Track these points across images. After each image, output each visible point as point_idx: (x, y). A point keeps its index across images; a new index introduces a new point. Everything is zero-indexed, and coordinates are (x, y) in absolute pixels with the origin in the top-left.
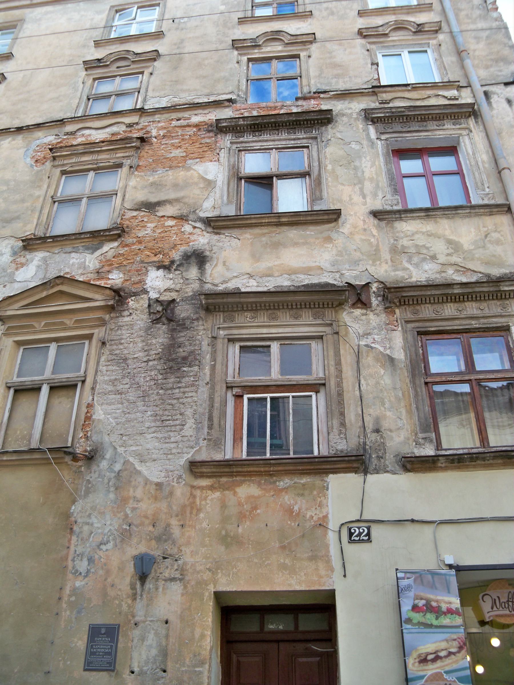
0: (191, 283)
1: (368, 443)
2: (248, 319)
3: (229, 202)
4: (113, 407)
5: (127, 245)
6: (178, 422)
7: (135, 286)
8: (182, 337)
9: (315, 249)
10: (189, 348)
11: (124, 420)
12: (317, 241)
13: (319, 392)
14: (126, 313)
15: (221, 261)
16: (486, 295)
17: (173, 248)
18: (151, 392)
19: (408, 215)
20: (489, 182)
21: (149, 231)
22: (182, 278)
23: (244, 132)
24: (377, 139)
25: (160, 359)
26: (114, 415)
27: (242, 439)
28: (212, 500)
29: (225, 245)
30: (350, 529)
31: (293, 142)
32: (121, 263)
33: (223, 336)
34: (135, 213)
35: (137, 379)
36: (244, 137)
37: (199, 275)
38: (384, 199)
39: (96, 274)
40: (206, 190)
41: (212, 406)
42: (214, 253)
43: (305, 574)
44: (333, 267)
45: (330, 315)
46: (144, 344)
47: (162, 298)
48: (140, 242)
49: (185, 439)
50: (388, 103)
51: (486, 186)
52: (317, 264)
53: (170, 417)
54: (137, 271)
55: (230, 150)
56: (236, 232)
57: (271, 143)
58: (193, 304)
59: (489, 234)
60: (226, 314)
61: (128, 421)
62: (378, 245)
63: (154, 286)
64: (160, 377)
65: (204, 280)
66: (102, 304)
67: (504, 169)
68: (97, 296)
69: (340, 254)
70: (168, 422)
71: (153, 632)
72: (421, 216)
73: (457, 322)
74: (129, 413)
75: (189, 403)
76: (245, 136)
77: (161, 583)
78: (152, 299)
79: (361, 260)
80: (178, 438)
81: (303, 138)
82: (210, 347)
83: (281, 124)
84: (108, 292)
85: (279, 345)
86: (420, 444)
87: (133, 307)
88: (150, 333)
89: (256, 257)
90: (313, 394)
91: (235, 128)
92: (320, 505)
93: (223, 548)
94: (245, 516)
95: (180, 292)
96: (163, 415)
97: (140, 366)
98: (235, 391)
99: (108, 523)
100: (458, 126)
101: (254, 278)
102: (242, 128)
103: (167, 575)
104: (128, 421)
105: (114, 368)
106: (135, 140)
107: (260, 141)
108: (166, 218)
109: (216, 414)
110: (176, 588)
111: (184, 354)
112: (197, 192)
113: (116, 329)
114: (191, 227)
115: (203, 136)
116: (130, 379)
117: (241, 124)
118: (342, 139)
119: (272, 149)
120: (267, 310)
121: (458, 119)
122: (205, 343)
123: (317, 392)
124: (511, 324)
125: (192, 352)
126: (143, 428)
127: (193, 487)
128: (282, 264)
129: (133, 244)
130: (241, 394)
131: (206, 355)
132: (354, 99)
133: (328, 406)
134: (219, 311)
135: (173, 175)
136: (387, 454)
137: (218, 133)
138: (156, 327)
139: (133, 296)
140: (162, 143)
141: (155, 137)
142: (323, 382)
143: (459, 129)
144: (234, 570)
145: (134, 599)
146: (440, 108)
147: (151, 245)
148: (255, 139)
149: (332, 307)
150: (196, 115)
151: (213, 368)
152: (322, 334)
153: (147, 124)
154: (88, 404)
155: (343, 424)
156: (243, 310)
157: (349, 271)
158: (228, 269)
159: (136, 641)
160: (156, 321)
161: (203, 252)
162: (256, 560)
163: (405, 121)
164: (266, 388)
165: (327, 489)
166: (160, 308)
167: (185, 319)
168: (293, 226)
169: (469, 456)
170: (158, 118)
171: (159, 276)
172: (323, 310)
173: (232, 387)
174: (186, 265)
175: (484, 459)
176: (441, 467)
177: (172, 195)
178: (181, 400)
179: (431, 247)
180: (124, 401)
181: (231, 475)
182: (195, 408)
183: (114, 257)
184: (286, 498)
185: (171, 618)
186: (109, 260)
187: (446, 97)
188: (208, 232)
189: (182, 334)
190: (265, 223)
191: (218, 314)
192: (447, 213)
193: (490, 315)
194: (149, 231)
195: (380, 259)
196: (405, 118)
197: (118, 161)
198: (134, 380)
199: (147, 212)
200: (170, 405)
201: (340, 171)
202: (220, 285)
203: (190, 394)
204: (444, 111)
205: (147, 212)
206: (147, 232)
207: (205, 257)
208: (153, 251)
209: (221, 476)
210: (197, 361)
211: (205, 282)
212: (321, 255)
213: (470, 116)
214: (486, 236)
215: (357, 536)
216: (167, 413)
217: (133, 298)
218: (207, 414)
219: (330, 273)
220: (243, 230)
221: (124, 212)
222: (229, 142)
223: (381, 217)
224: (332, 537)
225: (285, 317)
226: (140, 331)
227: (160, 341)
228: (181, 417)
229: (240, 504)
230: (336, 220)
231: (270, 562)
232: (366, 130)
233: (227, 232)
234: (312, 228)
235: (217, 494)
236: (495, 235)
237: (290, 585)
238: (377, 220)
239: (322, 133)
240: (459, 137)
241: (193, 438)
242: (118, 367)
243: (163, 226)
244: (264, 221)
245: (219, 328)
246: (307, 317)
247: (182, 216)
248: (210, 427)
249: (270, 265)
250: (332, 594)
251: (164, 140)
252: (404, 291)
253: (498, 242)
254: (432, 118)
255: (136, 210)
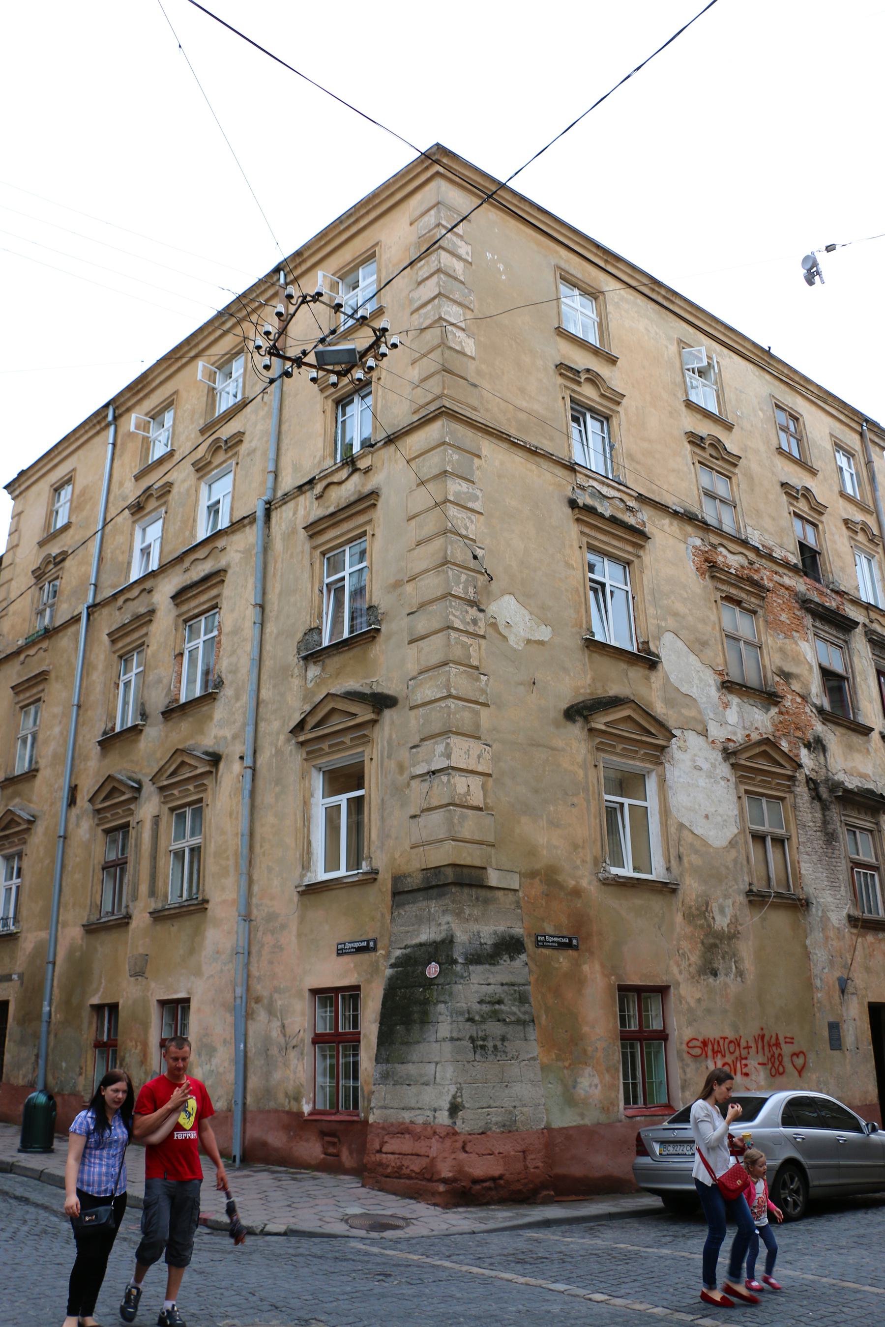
56: (833, 727)
148: (822, 627)
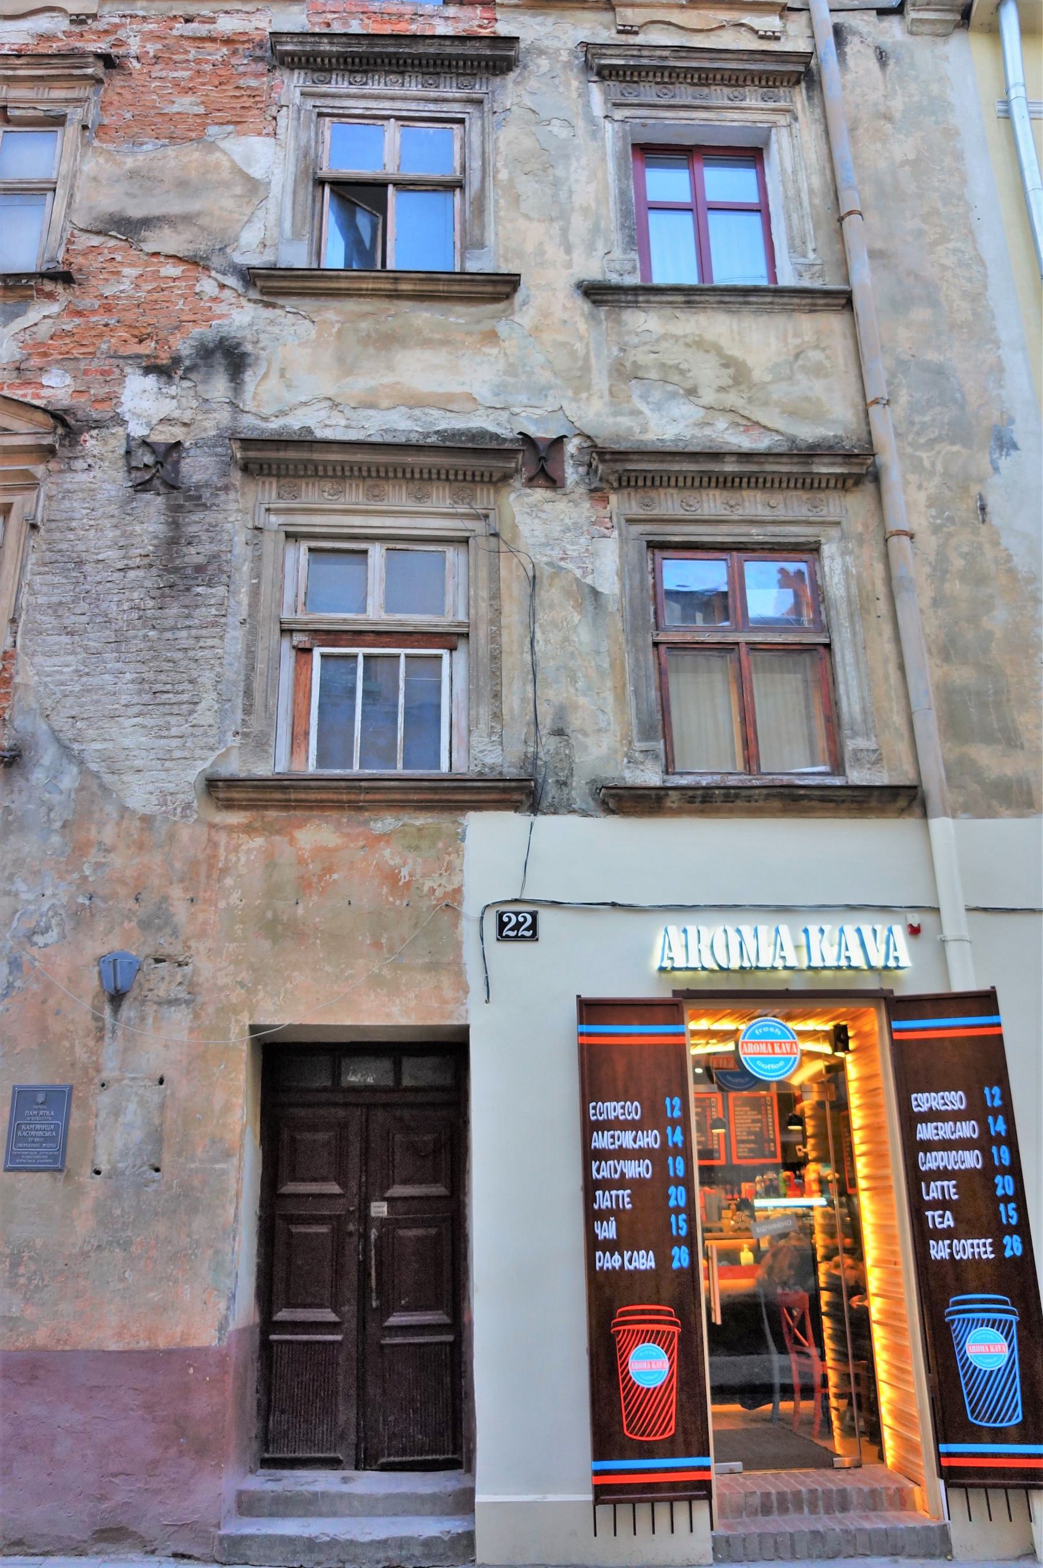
0: (215, 410)
1: (541, 755)
2: (326, 494)
3: (297, 235)
4: (56, 660)
5: (79, 313)
6: (185, 697)
7: (98, 406)
8: (195, 523)
9: (463, 355)
10: (208, 548)
11: (77, 688)
12: (469, 340)
13: (456, 649)
14: (80, 464)
15: (276, 367)
16: (785, 480)
17: (177, 328)
18: (132, 633)
19: (652, 298)
20: (816, 239)
21: (126, 285)
22: (197, 396)
23: (330, 70)
24: (606, 117)
25: (151, 566)
26: (58, 677)
27: (307, 734)
28: (249, 851)
29: (284, 333)
30: (500, 916)
31: (432, 107)
32: (68, 353)
33: (275, 527)
34: (96, 241)
35: (104, 606)
36: (329, 82)
37: (230, 394)
38: (608, 257)
39: (15, 374)
40: (248, 203)
41: (251, 668)
42: (263, 349)
43: (416, 996)
44: (495, 399)
45: (483, 498)
46: (118, 532)
47: (154, 438)
48: (108, 309)
49: (199, 731)
50: (636, 33)
51: (811, 246)
52: (466, 389)
53: (169, 687)
54: (103, 373)
55: (299, 111)
56: (307, 305)
57: (387, 104)
58: (217, 455)
59: (802, 352)
60: (283, 481)
61: (87, 690)
62: (586, 358)
63: (138, 411)
64: (151, 603)
65: (241, 406)
66: (29, 443)
67: (850, 213)
68: (17, 425)
69: (512, 370)
70: (166, 696)
71: (135, 1099)
72: (676, 302)
73: (724, 529)
74: (88, 674)
75: (207, 660)
76: (333, 82)
77: (150, 1009)
78: (134, 439)
79: (550, 388)
80: (185, 728)
81: (455, 100)
82: (250, 548)
83: (409, 61)
84: (40, 417)
85: (384, 551)
86: (635, 762)
87: (96, 452)
88: (129, 512)
89: (346, 367)
90: (445, 653)
91: (312, 60)
92: (450, 868)
93: (266, 944)
94: (309, 885)
95: (192, 428)
96: (156, 681)
97: (109, 579)
98: (299, 639)
99: (49, 892)
100: (771, 105)
101: (340, 408)
102: (327, 61)
103: (162, 993)
104: (87, 690)
105: (57, 579)
106: (91, 60)
107: (364, 97)
108: (162, 259)
109: (258, 684)
110: (180, 1016)
111: (200, 560)
112: (229, 203)
113: (60, 496)
114: (216, 284)
115: (241, 69)
116: (90, 604)
117: (324, 51)
118: (534, 111)
119: (387, 118)
120: (364, 478)
121: (775, 86)
122: (240, 538)
123: (452, 649)
124: (823, 540)
125: (214, 557)
126: (116, 706)
127: (212, 826)
128: (398, 383)
129: (94, 312)
130: (308, 646)
131: (243, 564)
132: (567, 13)
133: (472, 678)
134: (269, 475)
135: (176, 157)
136: (575, 779)
137: (274, 67)
138: (141, 500)
139: (94, 428)
140: (154, 75)
141: (137, 58)
142: (464, 630)
143: (774, 110)
144: (289, 986)
145: (100, 1039)
146: (740, 57)
147: (130, 317)
148: (354, 90)
149: (490, 481)
150: (227, 12)
151: (255, 592)
152: (467, 534)
153: (117, 20)
154: (5, 653)
155: (497, 716)
156: (316, 475)
157: (528, 409)
158: (289, 386)
159: (103, 1115)
160: (142, 487)
161: (239, 345)
162: (328, 968)
163: (666, 80)
164: (357, 637)
165: (463, 840)
166: (149, 459)
167: (202, 486)
168: (423, 301)
169: (722, 791)
170: (142, 9)
171: (149, 388)
172: (472, 485)
173: (291, 631)
174: (203, 369)
175: (749, 799)
176: (671, 808)
177: (174, 206)
178: (191, 653)
179: (689, 371)
180: (79, 650)
181: (286, 805)
182: (218, 670)
183: (52, 338)
184: (387, 853)
185: (170, 1074)
186: (42, 344)
187: (757, 32)
188: (249, 300)
189: (195, 517)
190: (367, 290)
191: (267, 480)
192: (727, 299)
193: (786, 519)
194: (126, 285)
195: (588, 387)
196: (666, 74)
197: (57, 109)
198: (97, 606)
199: (121, 240)
200: (169, 661)
201: (527, 186)
202: (273, 419)
203: (210, 642)
204: (747, 66)
205: (121, 240)
206: (122, 288)
207: (244, 355)
208: (136, 332)
209: (266, 808)
210: (225, 576)
211: (242, 411)
212: (475, 371)
213: (798, 82)
214: (797, 356)
215: (512, 929)
216: (163, 677)
217: (94, 432)
218: (242, 684)
219: (491, 411)
220: (322, 302)
221: (72, 235)
222: (298, 91)
223: (599, 297)
224: (468, 930)
225: (398, 497)
226: (110, 505)
227: (151, 529)
228: (190, 687)
229: (301, 861)
230: (508, 296)
231: (353, 972)
232: (584, 95)
233: (289, 303)
234: (460, 309)
235: (259, 841)
236: (815, 356)
237: (388, 1015)
238: (590, 304)
239: (493, 92)
240: (770, 129)
241: (214, 731)
242: (66, 577)
243: (156, 276)
244: (364, 286)
245: (268, 510)
246: (440, 499)
247: (195, 256)
248: (248, 710)
249: (373, 383)
250: (464, 1031)
251: (158, 67)
252: (630, 461)
253: (818, 371)
254: (722, 79)
255: (98, 233)
